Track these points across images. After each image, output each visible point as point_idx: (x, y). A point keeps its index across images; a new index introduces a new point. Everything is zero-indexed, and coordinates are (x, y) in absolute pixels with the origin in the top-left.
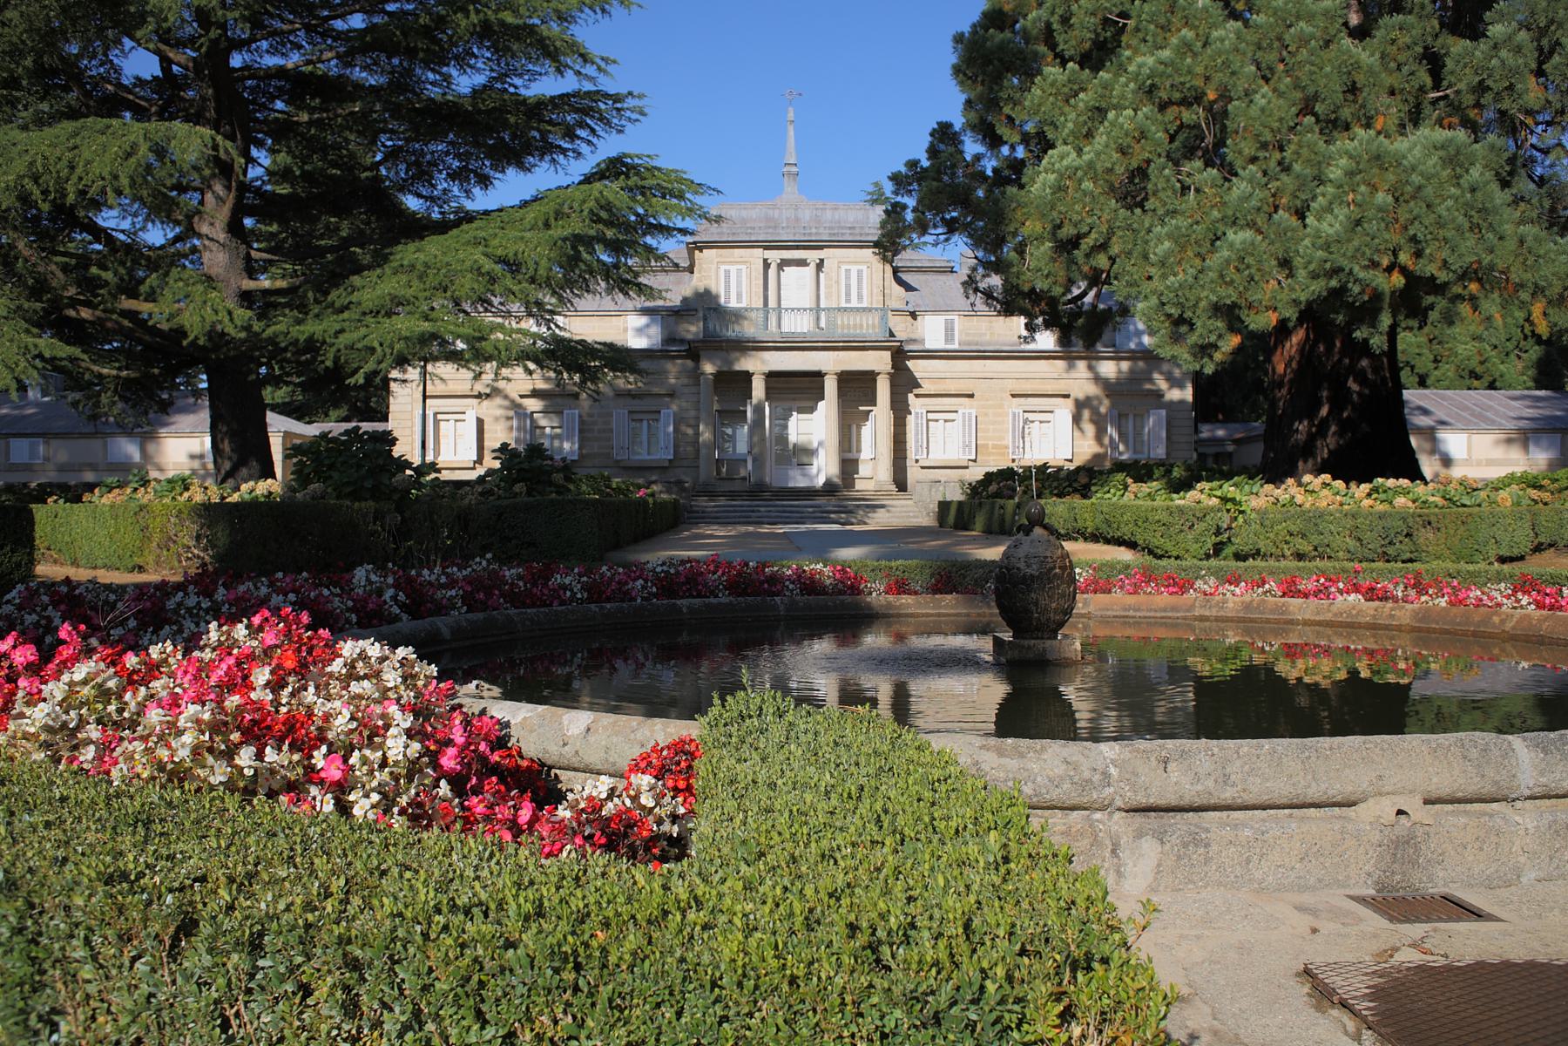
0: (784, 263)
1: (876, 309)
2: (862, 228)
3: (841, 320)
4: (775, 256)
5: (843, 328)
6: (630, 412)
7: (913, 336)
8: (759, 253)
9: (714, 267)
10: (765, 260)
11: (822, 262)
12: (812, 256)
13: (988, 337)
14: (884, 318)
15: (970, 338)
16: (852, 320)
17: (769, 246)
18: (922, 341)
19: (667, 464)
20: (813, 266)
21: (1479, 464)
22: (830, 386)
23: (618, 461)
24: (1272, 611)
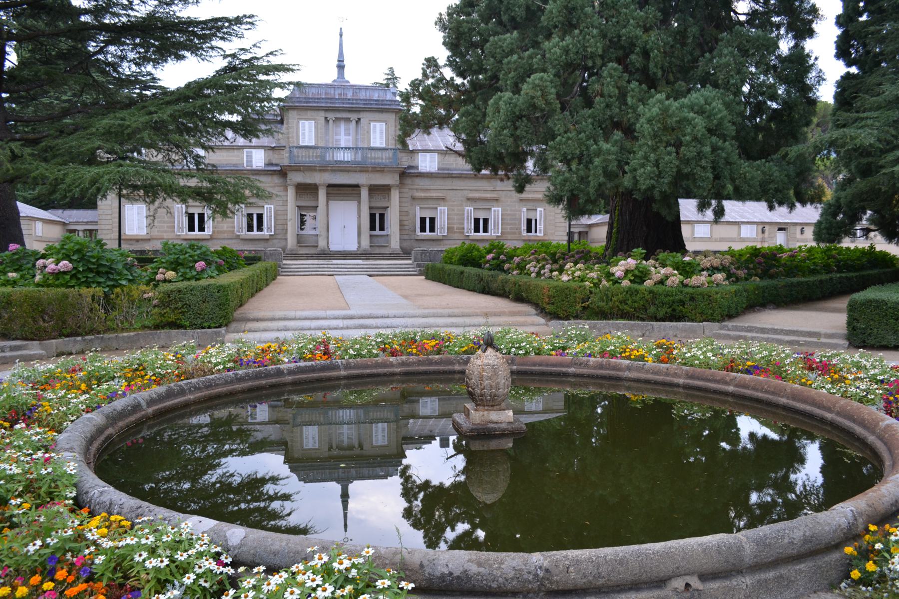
1: (391, 149)
2: (382, 101)
3: (370, 154)
4: (331, 116)
8: (322, 114)
9: (295, 121)
10: (326, 118)
11: (359, 119)
12: (354, 116)
13: (454, 166)
14: (394, 154)
15: (444, 166)
16: (377, 154)
17: (327, 110)
18: (417, 168)
19: (268, 237)
20: (354, 122)
21: (716, 241)
22: (364, 193)
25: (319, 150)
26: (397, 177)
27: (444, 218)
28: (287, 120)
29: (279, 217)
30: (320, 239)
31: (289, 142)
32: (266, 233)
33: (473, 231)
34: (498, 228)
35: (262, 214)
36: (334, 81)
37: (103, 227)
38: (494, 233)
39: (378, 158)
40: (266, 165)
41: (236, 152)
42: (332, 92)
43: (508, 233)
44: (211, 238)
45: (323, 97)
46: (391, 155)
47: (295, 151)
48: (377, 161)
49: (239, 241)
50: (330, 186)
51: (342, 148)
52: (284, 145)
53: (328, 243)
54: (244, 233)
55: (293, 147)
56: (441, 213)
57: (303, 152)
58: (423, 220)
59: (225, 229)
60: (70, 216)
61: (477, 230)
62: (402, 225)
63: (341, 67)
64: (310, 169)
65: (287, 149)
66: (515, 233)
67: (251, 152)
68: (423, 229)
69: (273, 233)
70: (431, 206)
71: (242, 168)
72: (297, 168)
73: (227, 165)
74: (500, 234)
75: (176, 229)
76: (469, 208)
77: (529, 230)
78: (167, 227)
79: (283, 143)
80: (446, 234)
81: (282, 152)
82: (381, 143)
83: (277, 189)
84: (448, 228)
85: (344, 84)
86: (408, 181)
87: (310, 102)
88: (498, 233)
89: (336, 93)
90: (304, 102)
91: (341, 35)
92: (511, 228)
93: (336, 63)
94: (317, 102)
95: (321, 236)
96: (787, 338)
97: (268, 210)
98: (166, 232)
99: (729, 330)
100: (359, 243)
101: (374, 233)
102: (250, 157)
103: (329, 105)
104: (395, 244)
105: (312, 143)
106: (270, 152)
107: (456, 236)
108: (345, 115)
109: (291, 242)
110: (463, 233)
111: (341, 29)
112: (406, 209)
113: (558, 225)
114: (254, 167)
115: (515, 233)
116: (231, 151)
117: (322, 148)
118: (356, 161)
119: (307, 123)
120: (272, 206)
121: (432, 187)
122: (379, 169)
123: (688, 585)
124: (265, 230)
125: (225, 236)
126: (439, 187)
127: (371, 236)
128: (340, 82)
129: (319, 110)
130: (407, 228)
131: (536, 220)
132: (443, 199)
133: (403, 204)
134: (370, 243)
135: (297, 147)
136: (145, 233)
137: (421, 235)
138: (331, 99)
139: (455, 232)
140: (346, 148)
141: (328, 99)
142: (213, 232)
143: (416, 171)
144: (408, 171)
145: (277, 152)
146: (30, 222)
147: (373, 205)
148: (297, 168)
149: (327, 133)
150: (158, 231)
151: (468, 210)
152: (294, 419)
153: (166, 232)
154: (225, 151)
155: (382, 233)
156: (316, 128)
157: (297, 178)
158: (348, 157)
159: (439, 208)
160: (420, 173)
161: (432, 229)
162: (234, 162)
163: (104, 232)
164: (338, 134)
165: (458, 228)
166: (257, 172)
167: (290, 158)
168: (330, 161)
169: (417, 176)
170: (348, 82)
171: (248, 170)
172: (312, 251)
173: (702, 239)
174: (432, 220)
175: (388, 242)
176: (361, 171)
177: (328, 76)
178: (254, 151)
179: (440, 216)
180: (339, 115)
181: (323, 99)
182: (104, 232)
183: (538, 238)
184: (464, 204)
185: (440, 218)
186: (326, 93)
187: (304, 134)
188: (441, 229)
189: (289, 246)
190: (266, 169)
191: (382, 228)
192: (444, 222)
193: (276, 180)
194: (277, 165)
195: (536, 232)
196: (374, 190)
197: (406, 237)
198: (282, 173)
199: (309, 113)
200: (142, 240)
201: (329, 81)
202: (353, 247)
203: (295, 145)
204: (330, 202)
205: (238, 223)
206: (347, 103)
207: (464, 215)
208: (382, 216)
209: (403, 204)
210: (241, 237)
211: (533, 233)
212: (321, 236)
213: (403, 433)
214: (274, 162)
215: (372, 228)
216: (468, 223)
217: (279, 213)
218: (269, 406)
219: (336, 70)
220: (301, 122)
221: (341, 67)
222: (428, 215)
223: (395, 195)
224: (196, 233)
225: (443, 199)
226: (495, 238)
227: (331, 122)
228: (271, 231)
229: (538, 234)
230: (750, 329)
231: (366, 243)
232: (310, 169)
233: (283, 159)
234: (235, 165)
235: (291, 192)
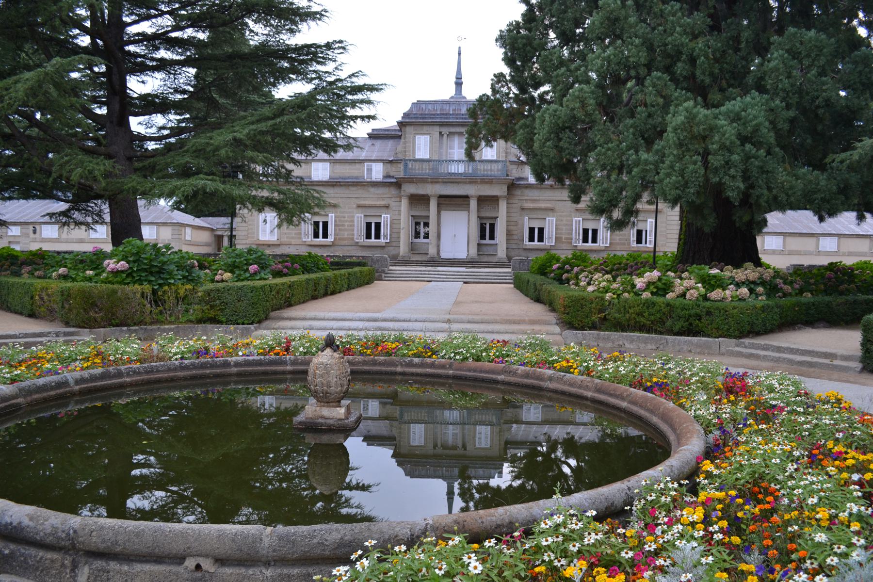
0: (451, 134)
4: (445, 130)
5: (484, 171)
6: (365, 216)
7: (522, 176)
8: (437, 129)
9: (412, 136)
10: (440, 133)
17: (442, 125)
19: (384, 245)
22: (473, 204)
23: (358, 242)
24: (522, 376)
25: (431, 163)
26: (505, 188)
27: (552, 228)
28: (405, 135)
29: (395, 226)
30: (430, 247)
31: (406, 155)
32: (382, 241)
33: (581, 241)
34: (607, 239)
35: (380, 223)
36: (452, 97)
37: (240, 233)
38: (603, 243)
39: (488, 170)
40: (384, 177)
41: (357, 166)
42: (448, 108)
43: (618, 244)
44: (333, 244)
45: (439, 113)
46: (500, 167)
47: (410, 165)
48: (489, 173)
49: (358, 247)
50: (441, 197)
51: (453, 161)
52: (401, 158)
53: (438, 251)
54: (363, 241)
55: (407, 160)
56: (549, 224)
57: (418, 165)
58: (532, 230)
59: (346, 236)
60: (218, 223)
61: (585, 240)
62: (509, 234)
63: (459, 84)
64: (423, 180)
65: (403, 163)
66: (624, 244)
67: (371, 166)
68: (531, 239)
69: (388, 241)
70: (540, 217)
71: (363, 180)
72: (411, 180)
73: (349, 178)
74: (608, 245)
75: (303, 236)
76: (578, 219)
77: (639, 241)
78: (295, 234)
79: (400, 157)
80: (553, 244)
81: (399, 165)
82: (492, 156)
83: (393, 199)
84: (556, 238)
85: (459, 100)
86: (518, 192)
87: (426, 118)
88: (606, 243)
89: (451, 109)
90: (420, 118)
91: (459, 54)
92: (620, 239)
93: (455, 80)
94: (433, 118)
95: (431, 244)
96: (799, 358)
97: (385, 218)
98: (293, 238)
99: (746, 347)
100: (468, 251)
101: (484, 242)
102: (370, 170)
103: (443, 120)
104: (501, 253)
105: (427, 157)
106: (389, 165)
107: (564, 246)
108: (458, 129)
109: (403, 249)
110: (571, 243)
111: (460, 48)
112: (515, 219)
113: (669, 236)
114: (374, 179)
115: (624, 244)
116: (353, 164)
117: (434, 161)
118: (466, 174)
119: (422, 137)
120: (389, 216)
121: (541, 198)
122: (488, 180)
123: (198, 567)
124: (382, 237)
125: (345, 242)
126: (548, 198)
127: (479, 245)
128: (456, 98)
129: (433, 125)
130: (515, 237)
131: (646, 231)
132: (552, 210)
133: (513, 215)
134: (478, 250)
135: (410, 160)
136: (276, 239)
137: (529, 245)
138: (446, 114)
139: (563, 243)
140: (456, 161)
141: (443, 114)
142: (335, 239)
143: (525, 182)
144: (518, 183)
145: (395, 165)
146: (180, 228)
147: (483, 214)
148: (411, 180)
149: (440, 147)
150: (287, 238)
151: (576, 221)
152: (402, 415)
153: (293, 238)
154: (347, 164)
155: (492, 242)
156: (431, 142)
157: (410, 189)
158: (461, 169)
159: (547, 219)
160: (530, 184)
161: (541, 239)
162: (356, 175)
163: (241, 237)
164: (452, 148)
165: (566, 238)
166: (375, 184)
167: (405, 170)
168: (442, 173)
169: (526, 187)
170: (465, 98)
171: (368, 182)
172: (425, 258)
173: (828, 253)
174: (541, 231)
175: (496, 252)
176: (470, 183)
177: (446, 92)
178: (374, 164)
179: (549, 226)
180: (453, 130)
181: (438, 114)
182: (241, 237)
183: (647, 250)
184: (573, 214)
185: (549, 229)
186: (441, 110)
187: (419, 148)
188: (549, 240)
189: (401, 254)
190: (385, 181)
191: (492, 237)
192: (552, 232)
193: (393, 191)
194: (393, 177)
195: (646, 243)
196: (483, 200)
197: (514, 246)
198: (398, 185)
199: (425, 128)
200: (273, 245)
201: (446, 97)
202: (462, 255)
203: (411, 158)
204: (443, 213)
205: (358, 231)
206: (460, 118)
207: (572, 225)
208: (492, 227)
209: (513, 215)
210: (360, 244)
211: (643, 244)
212: (431, 244)
213: (507, 436)
214: (392, 174)
215: (483, 237)
216: (576, 233)
217: (395, 222)
218: (380, 403)
219: (454, 86)
220: (417, 136)
221: (459, 84)
222: (536, 225)
223: (503, 206)
224: (321, 240)
225: (552, 210)
226: (604, 248)
227: (445, 136)
228: (387, 239)
229: (648, 245)
230: (779, 349)
231: (474, 251)
232: (423, 180)
233: (398, 172)
234: (357, 178)
235: (404, 203)
